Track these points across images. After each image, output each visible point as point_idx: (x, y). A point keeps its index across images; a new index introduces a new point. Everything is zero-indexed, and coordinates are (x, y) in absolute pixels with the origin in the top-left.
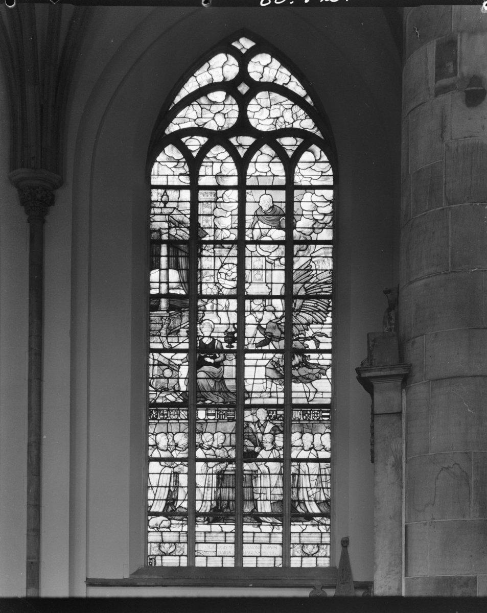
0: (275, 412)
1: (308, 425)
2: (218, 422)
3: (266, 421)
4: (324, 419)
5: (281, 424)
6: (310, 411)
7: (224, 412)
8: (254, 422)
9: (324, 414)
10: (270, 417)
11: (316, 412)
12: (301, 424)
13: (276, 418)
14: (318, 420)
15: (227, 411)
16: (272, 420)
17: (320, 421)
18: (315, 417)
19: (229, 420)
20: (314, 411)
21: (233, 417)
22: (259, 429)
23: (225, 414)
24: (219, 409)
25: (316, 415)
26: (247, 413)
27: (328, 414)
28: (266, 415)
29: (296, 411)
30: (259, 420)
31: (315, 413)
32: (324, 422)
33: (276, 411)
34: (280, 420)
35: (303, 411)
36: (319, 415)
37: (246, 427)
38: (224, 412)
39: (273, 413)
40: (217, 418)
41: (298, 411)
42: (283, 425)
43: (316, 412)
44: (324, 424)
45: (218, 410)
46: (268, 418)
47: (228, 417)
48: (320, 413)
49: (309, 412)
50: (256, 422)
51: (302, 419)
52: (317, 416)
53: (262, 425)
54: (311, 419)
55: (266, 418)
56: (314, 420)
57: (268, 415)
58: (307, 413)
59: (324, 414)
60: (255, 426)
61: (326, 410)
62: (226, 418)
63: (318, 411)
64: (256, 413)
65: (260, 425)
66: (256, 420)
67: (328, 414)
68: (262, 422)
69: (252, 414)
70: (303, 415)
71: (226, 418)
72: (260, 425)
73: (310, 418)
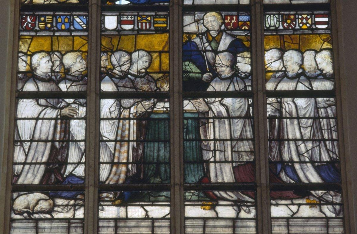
0: (235, 17)
1: (292, 36)
2: (138, 34)
3: (220, 32)
4: (319, 27)
5: (245, 36)
6: (295, 15)
7: (149, 18)
8: (200, 34)
9: (317, 19)
10: (227, 25)
11: (305, 16)
12: (280, 35)
13: (237, 27)
14: (309, 29)
15: (154, 17)
16: (231, 30)
17: (313, 30)
18: (303, 24)
19: (158, 31)
20: (301, 15)
21: (165, 25)
22: (210, 45)
23: (150, 22)
24: (141, 13)
25: (304, 21)
26: (187, 19)
27: (326, 19)
28: (220, 22)
29: (270, 15)
30: (208, 31)
31: (302, 19)
32: (319, 32)
33: (237, 16)
34: (245, 30)
35: (282, 15)
36: (310, 21)
37: (187, 42)
38: (149, 18)
39: (232, 19)
40: (136, 28)
41: (274, 15)
42: (249, 38)
43: (305, 16)
44: (319, 34)
45: (138, 15)
46: (223, 27)
47: (155, 25)
48: (311, 17)
49: (292, 17)
50: (203, 34)
51: (281, 27)
52: (308, 23)
53: (214, 38)
54: (297, 27)
55: (220, 26)
56: (301, 29)
57: (223, 23)
58: (290, 19)
59: (317, 19)
60: (201, 39)
61: (322, 12)
62: (152, 28)
63: (308, 15)
64: (203, 19)
65: (211, 38)
66: (203, 29)
67: (326, 19)
68: (214, 34)
69: (197, 21)
70: (284, 21)
71: (152, 28)
72: (211, 38)
73: (295, 25)
